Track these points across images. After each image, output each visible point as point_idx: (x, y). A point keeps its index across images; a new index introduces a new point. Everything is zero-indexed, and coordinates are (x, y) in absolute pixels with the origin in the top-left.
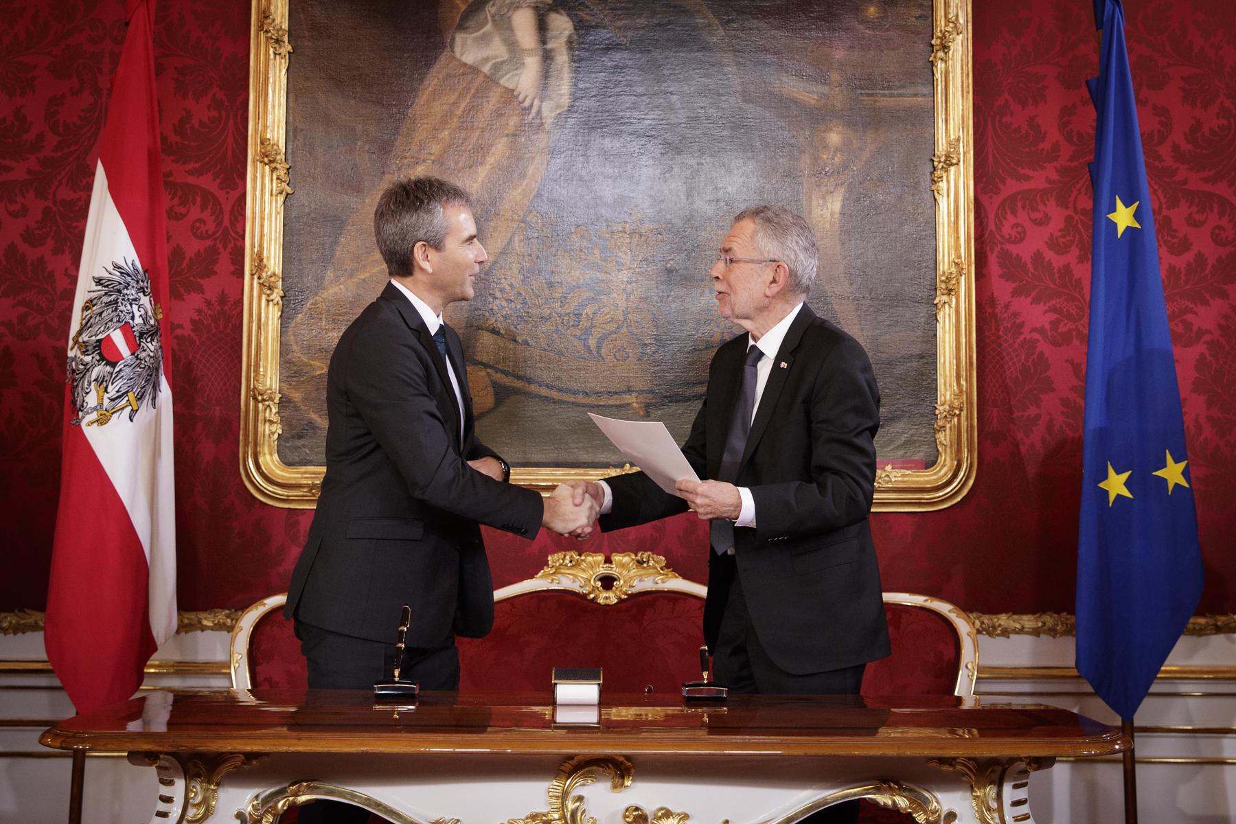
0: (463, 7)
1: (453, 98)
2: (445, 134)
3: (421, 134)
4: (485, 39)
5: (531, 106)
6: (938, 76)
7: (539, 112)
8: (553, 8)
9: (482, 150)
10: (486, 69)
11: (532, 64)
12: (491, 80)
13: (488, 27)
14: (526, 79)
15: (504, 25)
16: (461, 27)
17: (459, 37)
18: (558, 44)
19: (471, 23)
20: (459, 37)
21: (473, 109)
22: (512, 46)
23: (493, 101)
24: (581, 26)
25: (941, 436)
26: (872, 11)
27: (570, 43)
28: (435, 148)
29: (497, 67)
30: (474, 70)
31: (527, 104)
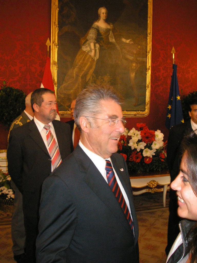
1: (82, 56)
2: (81, 61)
4: (87, 47)
5: (93, 57)
6: (148, 57)
7: (94, 58)
8: (96, 43)
10: (87, 52)
11: (93, 51)
12: (88, 53)
13: (87, 45)
14: (92, 54)
15: (89, 45)
16: (83, 45)
17: (83, 46)
18: (97, 48)
20: (83, 46)
21: (85, 57)
22: (91, 48)
23: (88, 56)
24: (100, 46)
25: (146, 107)
27: (99, 49)
29: (88, 52)
30: (85, 52)
31: (92, 57)
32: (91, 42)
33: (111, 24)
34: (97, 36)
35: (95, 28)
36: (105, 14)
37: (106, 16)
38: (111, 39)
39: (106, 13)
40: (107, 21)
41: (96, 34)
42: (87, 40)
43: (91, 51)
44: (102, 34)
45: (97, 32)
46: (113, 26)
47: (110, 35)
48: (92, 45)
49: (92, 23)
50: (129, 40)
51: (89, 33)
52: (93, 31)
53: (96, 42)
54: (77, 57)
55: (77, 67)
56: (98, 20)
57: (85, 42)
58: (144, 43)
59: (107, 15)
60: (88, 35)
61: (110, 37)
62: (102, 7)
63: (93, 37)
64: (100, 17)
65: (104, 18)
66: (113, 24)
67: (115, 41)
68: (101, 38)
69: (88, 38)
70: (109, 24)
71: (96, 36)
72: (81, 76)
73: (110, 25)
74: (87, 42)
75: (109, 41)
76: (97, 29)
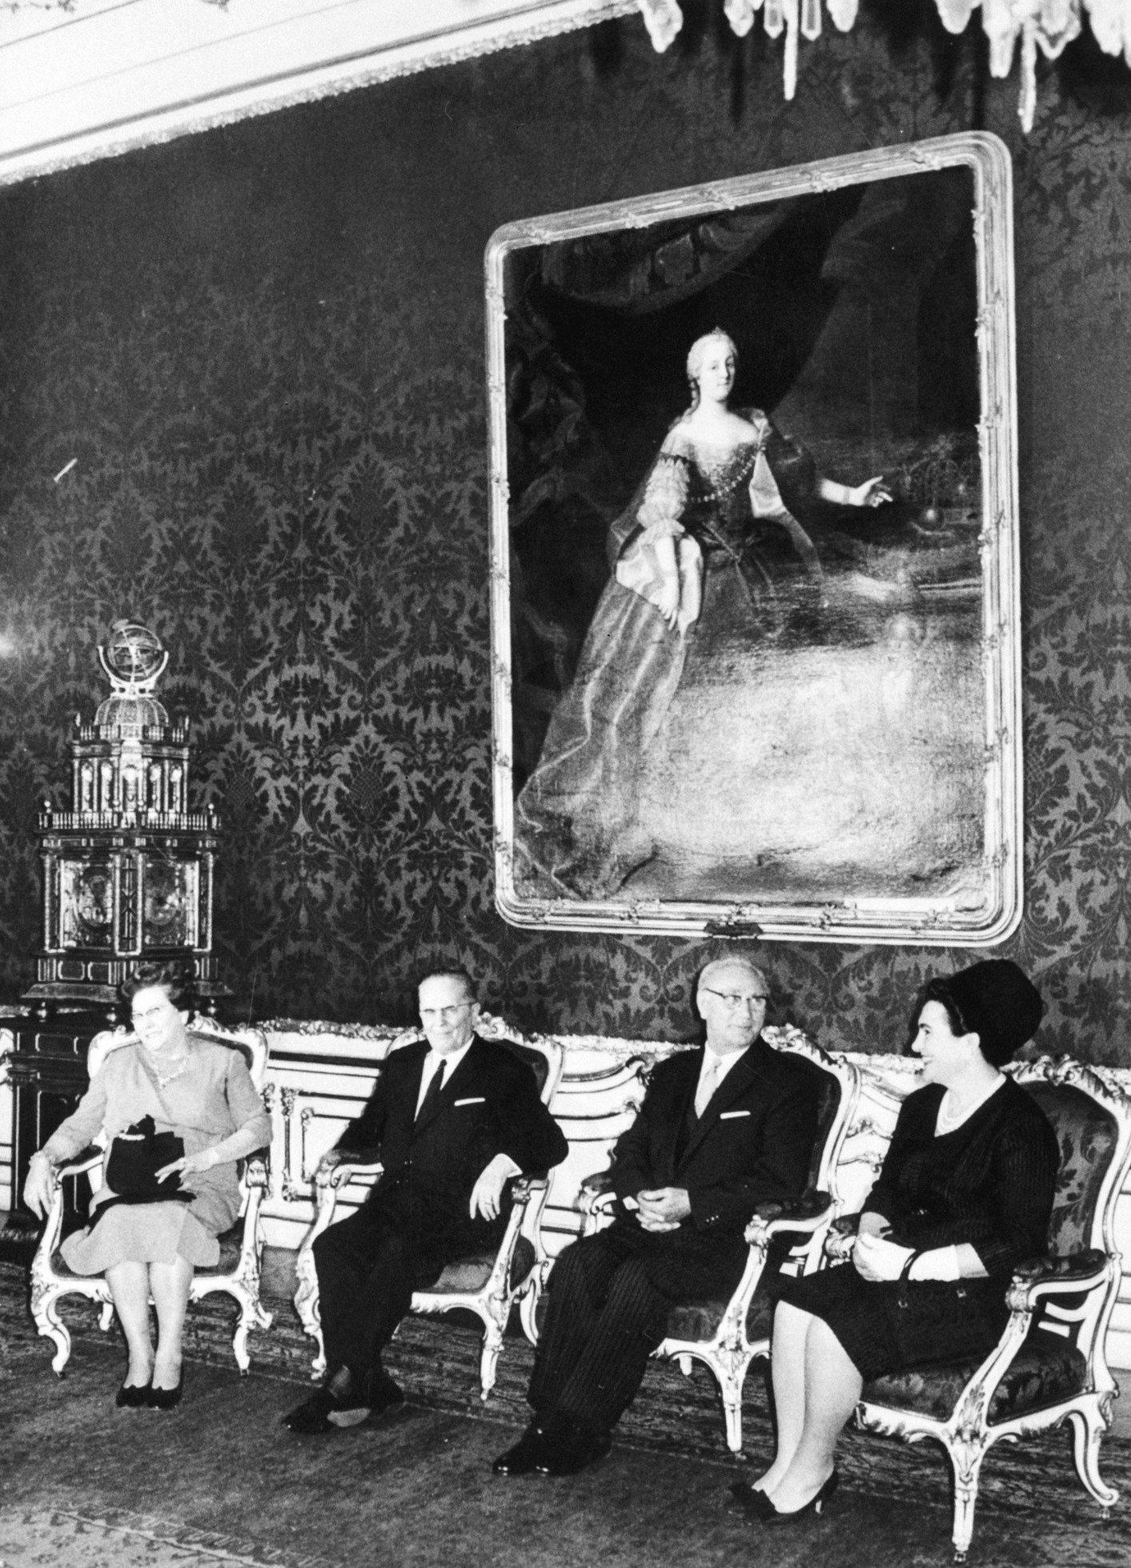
0: (622, 541)
1: (615, 614)
3: (597, 644)
8: (684, 536)
9: (639, 654)
11: (672, 582)
16: (621, 557)
19: (627, 554)
20: (620, 565)
22: (657, 572)
24: (706, 550)
26: (931, 514)
28: (608, 656)
29: (646, 589)
30: (630, 592)
32: (657, 537)
33: (759, 416)
34: (689, 495)
35: (676, 458)
36: (723, 372)
37: (728, 378)
38: (761, 498)
39: (731, 360)
40: (738, 402)
41: (684, 489)
42: (640, 529)
43: (659, 581)
44: (714, 480)
45: (687, 478)
46: (771, 424)
47: (753, 482)
48: (665, 547)
49: (663, 433)
50: (866, 487)
51: (649, 488)
52: (669, 472)
53: (682, 529)
54: (595, 626)
55: (597, 673)
56: (688, 411)
57: (630, 541)
58: (961, 488)
59: (732, 371)
60: (642, 502)
61: (754, 487)
62: (708, 330)
63: (666, 507)
64: (698, 388)
65: (723, 391)
66: (767, 415)
67: (784, 509)
68: (710, 501)
69: (643, 516)
70: (747, 418)
71: (684, 499)
72: (616, 720)
73: (751, 422)
74: (641, 540)
75: (751, 515)
76: (684, 460)
